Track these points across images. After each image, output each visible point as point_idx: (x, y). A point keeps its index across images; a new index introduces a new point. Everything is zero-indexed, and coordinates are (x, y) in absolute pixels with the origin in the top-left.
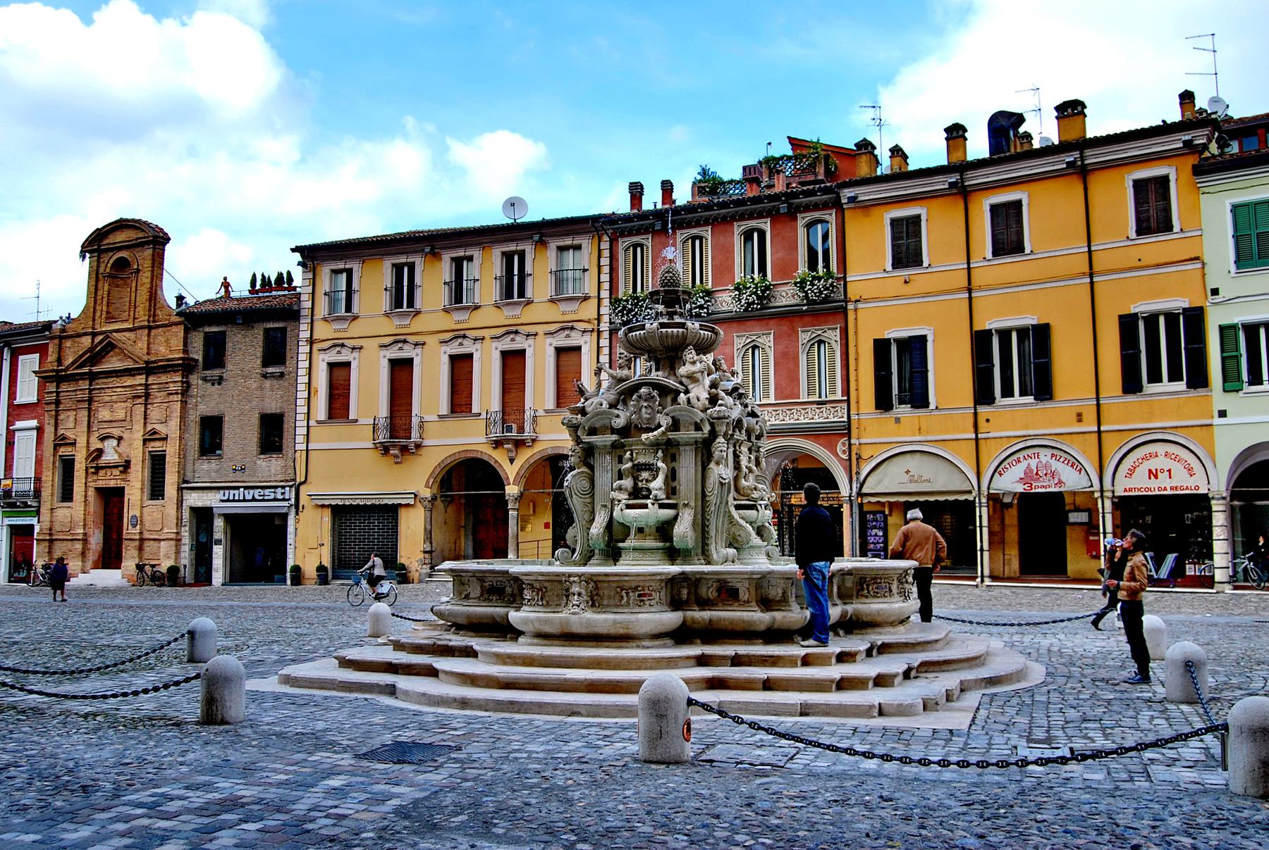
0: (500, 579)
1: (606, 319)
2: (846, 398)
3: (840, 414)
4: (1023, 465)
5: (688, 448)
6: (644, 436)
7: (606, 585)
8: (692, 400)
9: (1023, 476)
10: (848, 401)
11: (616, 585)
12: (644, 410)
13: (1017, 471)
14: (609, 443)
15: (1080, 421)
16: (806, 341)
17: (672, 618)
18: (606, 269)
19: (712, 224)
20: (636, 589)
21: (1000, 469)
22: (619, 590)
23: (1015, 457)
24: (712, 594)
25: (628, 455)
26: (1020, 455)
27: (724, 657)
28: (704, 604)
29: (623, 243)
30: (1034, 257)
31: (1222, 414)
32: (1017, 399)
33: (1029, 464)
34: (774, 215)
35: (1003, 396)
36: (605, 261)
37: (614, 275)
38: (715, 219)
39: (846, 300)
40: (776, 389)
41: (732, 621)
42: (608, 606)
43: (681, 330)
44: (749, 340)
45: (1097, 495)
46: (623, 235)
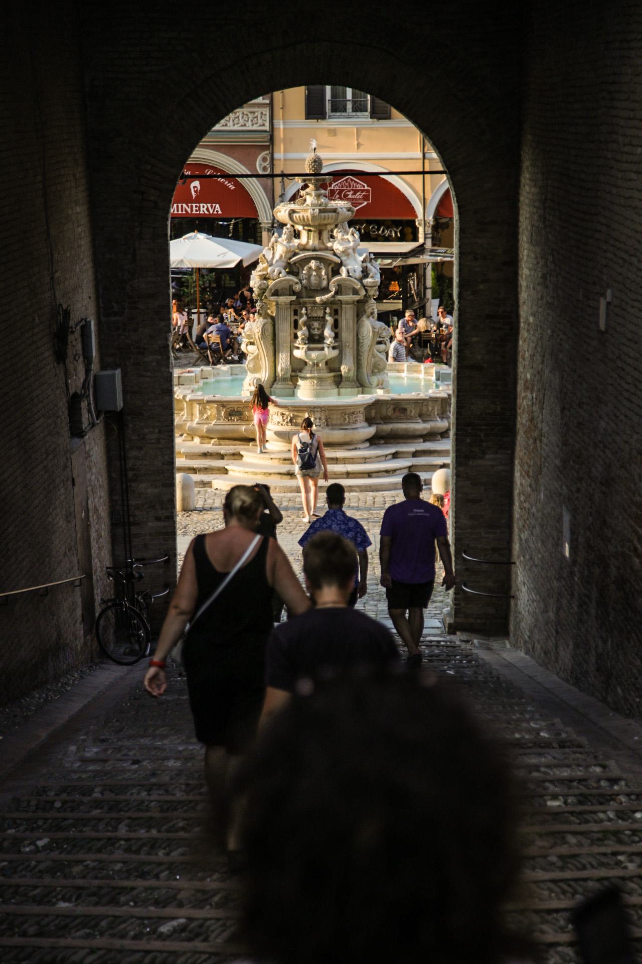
2: (267, 101)
3: (260, 121)
5: (348, 306)
7: (335, 412)
8: (350, 271)
14: (289, 301)
17: (371, 431)
20: (353, 413)
22: (343, 414)
25: (304, 311)
27: (407, 453)
28: (386, 420)
41: (406, 430)
42: (336, 425)
43: (334, 214)
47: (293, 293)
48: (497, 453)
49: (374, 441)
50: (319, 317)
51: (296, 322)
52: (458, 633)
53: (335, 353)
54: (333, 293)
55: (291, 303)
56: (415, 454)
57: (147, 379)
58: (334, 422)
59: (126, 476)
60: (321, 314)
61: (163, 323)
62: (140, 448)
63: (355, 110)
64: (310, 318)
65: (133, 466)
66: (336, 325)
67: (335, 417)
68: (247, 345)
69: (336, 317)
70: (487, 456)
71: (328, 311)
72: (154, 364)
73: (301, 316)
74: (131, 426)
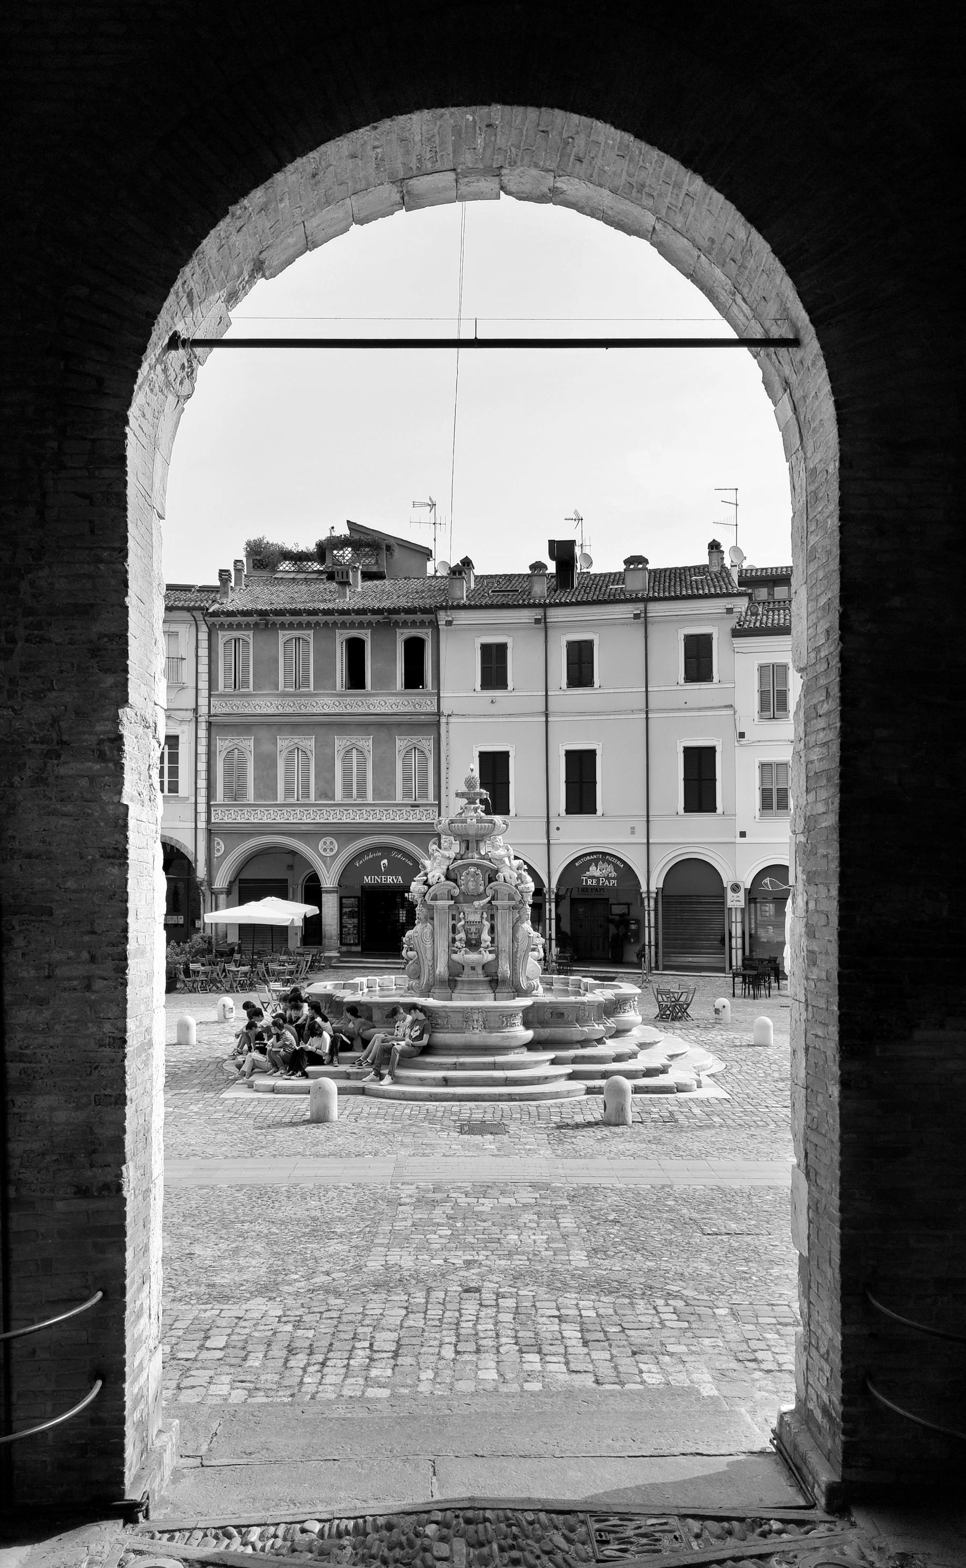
1: (203, 710)
6: (476, 903)
10: (439, 805)
12: (470, 883)
15: (633, 833)
18: (204, 660)
19: (315, 628)
24: (547, 1016)
29: (223, 636)
30: (602, 691)
31: (743, 834)
34: (375, 627)
36: (203, 652)
37: (213, 667)
38: (317, 624)
39: (439, 714)
44: (349, 743)
45: (644, 895)
46: (222, 626)
47: (452, 898)
48: (942, 1026)
51: (454, 927)
53: (491, 957)
54: (489, 898)
55: (450, 906)
58: (492, 1025)
61: (110, 680)
62: (42, 1002)
66: (492, 930)
67: (492, 1019)
70: (918, 1035)
71: (485, 915)
72: (84, 782)
73: (460, 921)
74: (19, 942)
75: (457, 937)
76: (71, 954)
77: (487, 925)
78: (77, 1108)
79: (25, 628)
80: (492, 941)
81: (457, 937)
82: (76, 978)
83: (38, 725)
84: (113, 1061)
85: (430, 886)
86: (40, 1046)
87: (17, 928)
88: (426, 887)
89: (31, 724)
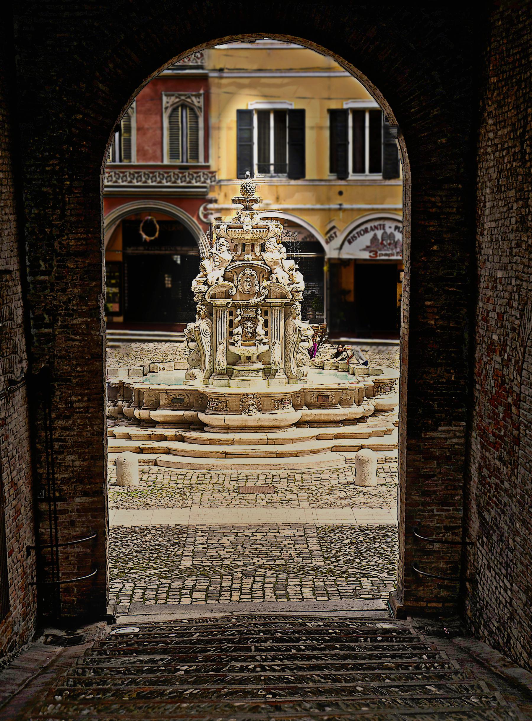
0: (180, 393)
4: (370, 235)
9: (369, 244)
11: (271, 398)
13: (366, 240)
16: (169, 105)
21: (349, 237)
22: (273, 401)
23: (363, 227)
24: (313, 400)
25: (239, 312)
26: (368, 226)
32: (368, 176)
33: (375, 235)
35: (354, 171)
40: (138, 151)
49: (299, 424)
50: (251, 318)
52: (408, 618)
54: (263, 297)
56: (336, 437)
57: (76, 343)
58: (265, 408)
59: (52, 447)
60: (252, 314)
63: (276, 171)
64: (244, 318)
65: (59, 436)
67: (265, 403)
68: (188, 342)
69: (266, 317)
70: (440, 428)
74: (58, 393)
75: (235, 331)
76: (80, 398)
77: (261, 320)
78: (83, 461)
79: (57, 262)
80: (266, 334)
81: (235, 331)
82: (82, 408)
83: (63, 303)
84: (98, 441)
85: (209, 287)
86: (68, 436)
87: (57, 387)
88: (206, 287)
89: (60, 303)
